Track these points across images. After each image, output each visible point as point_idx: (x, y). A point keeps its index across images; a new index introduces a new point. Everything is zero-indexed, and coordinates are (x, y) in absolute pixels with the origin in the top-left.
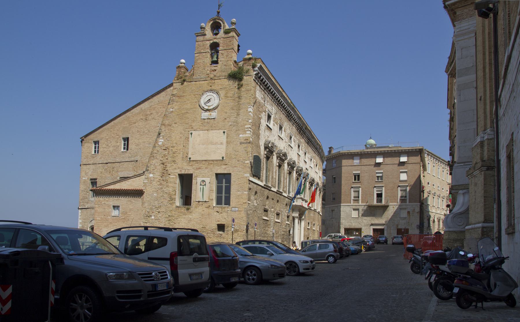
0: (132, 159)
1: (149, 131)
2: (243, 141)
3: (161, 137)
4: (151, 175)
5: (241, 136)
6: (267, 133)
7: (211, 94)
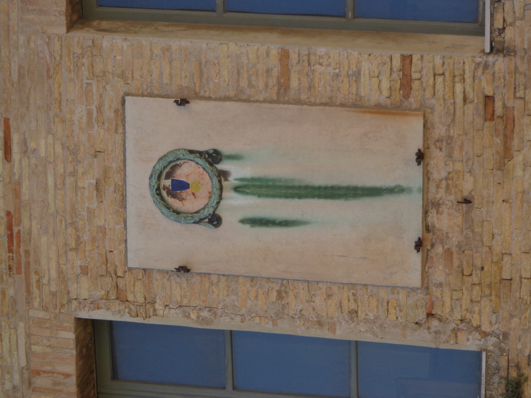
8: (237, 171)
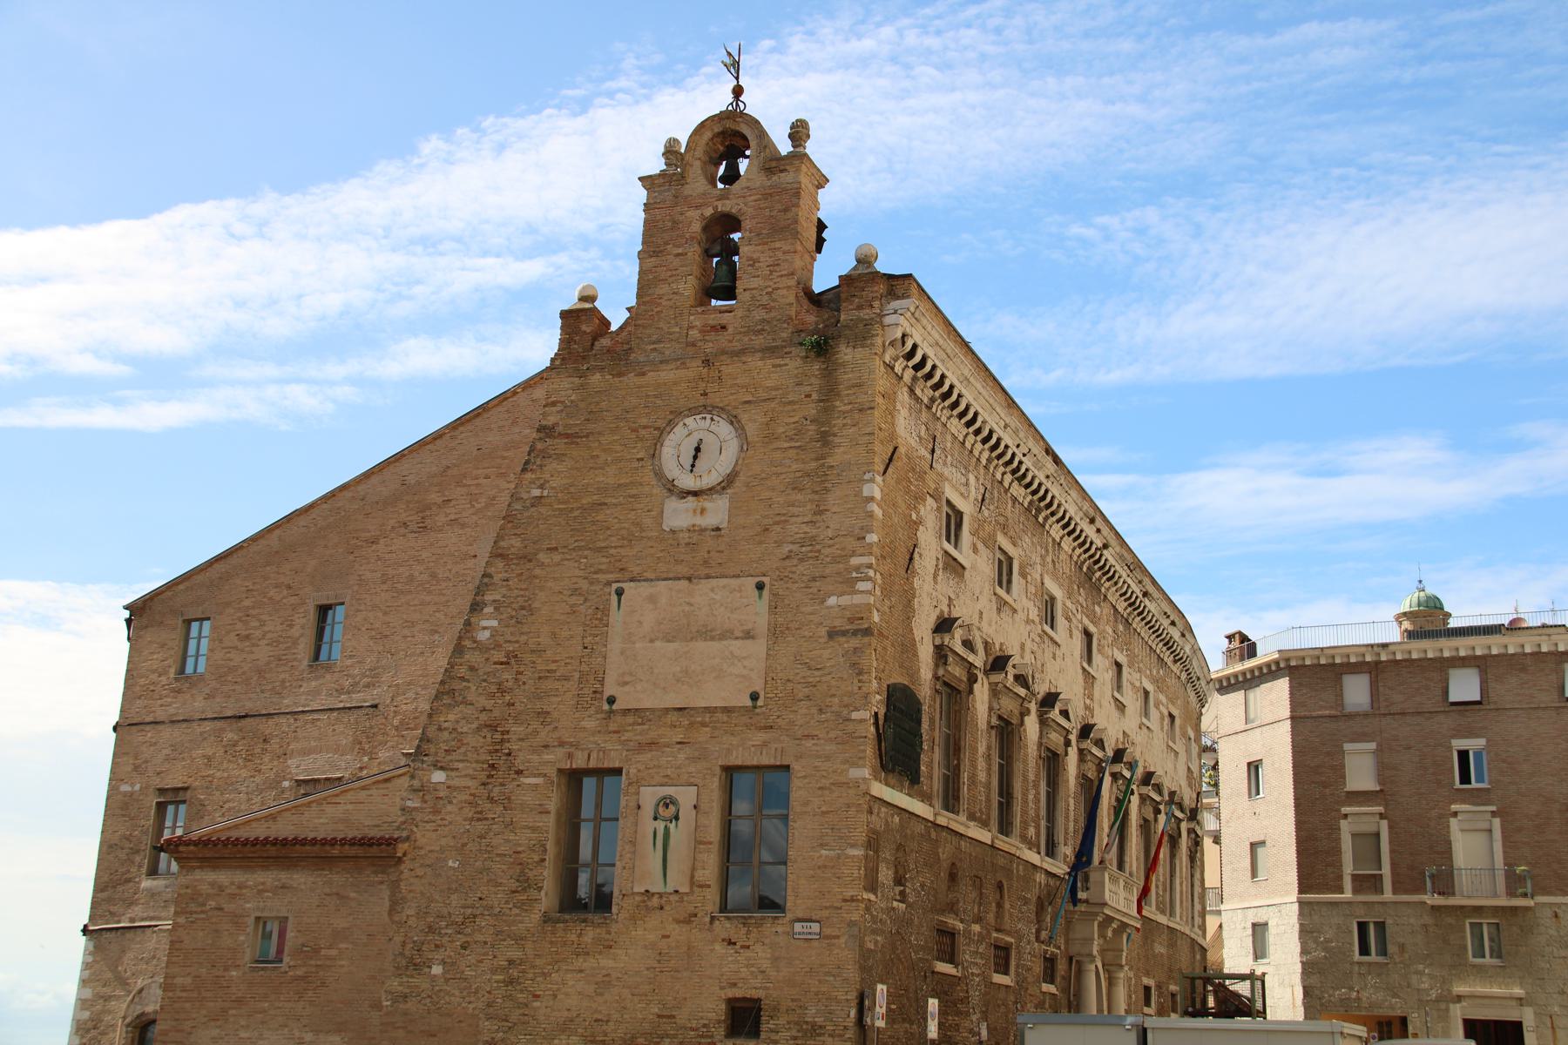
0: (356, 699)
1: (434, 576)
2: (837, 623)
3: (489, 610)
4: (438, 777)
5: (832, 601)
6: (946, 586)
7: (702, 424)
8: (672, 826)
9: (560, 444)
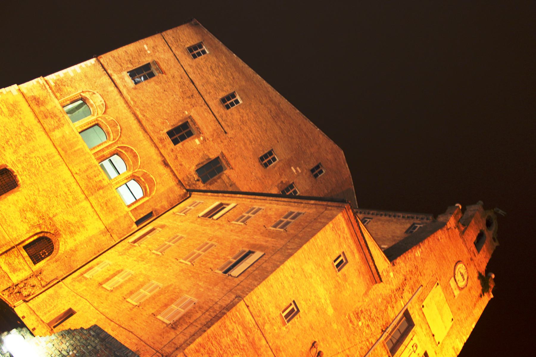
2: (456, 347)
4: (391, 274)
9: (447, 235)
